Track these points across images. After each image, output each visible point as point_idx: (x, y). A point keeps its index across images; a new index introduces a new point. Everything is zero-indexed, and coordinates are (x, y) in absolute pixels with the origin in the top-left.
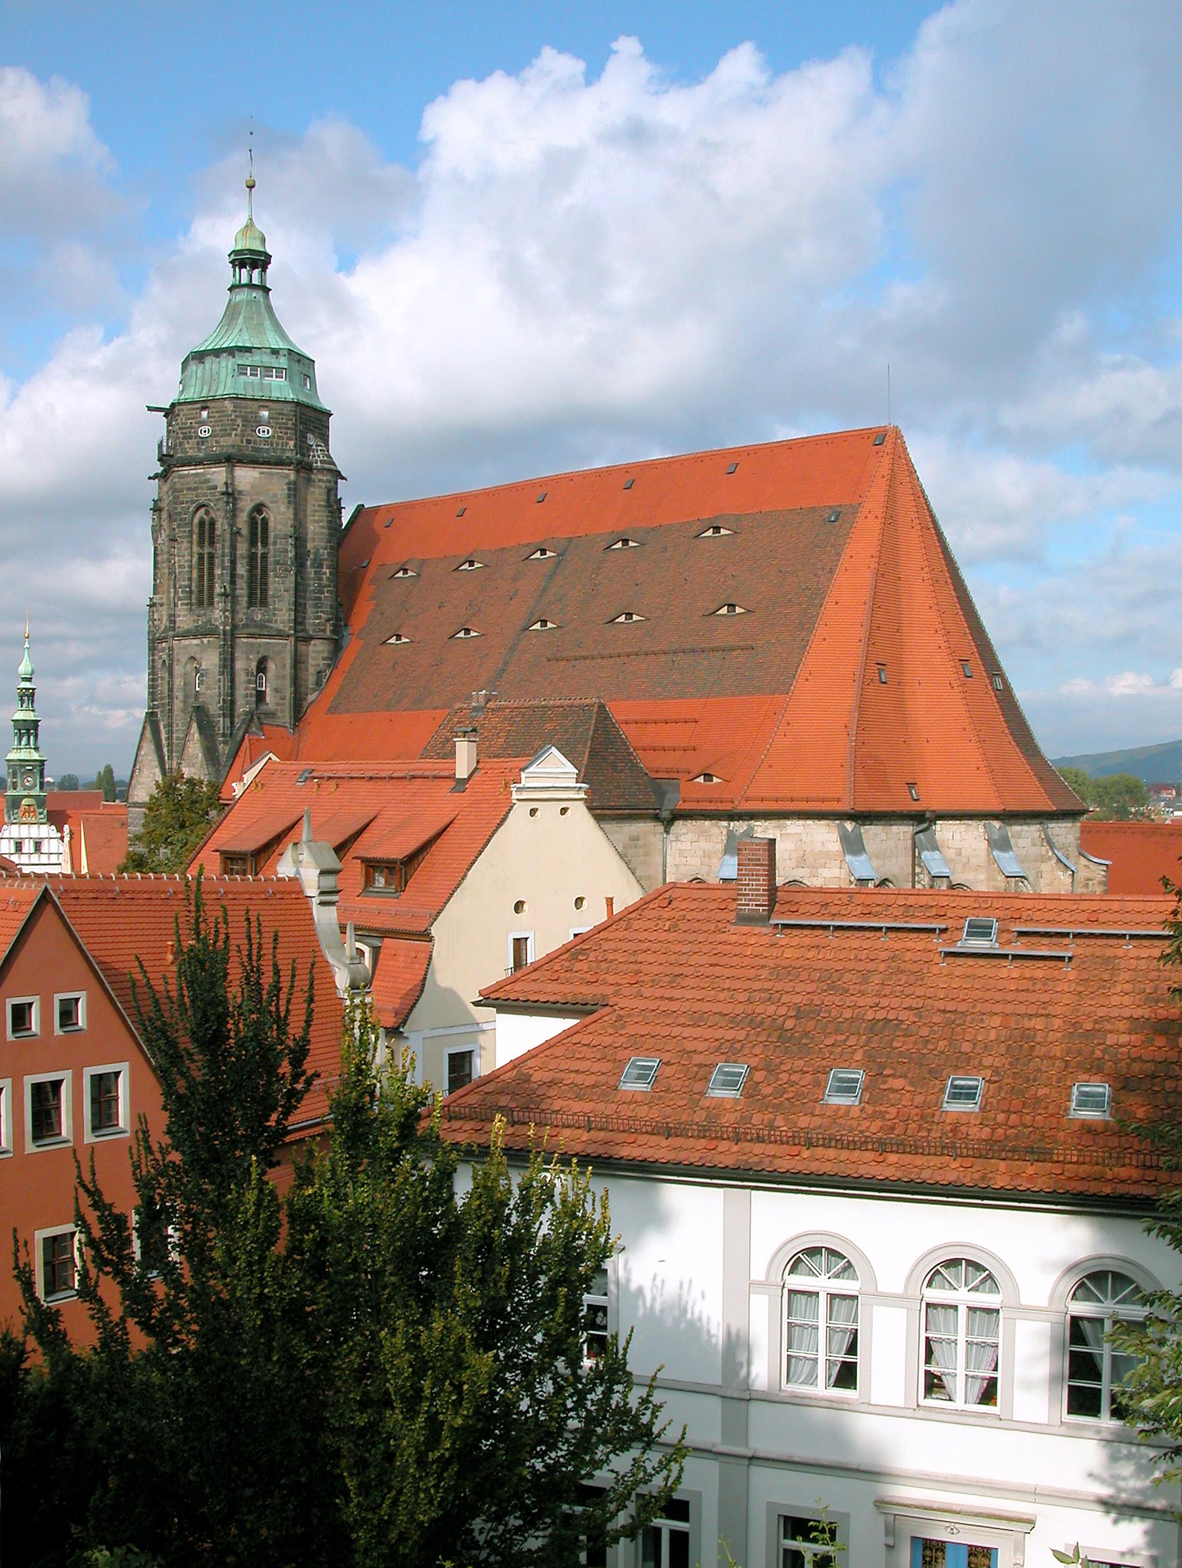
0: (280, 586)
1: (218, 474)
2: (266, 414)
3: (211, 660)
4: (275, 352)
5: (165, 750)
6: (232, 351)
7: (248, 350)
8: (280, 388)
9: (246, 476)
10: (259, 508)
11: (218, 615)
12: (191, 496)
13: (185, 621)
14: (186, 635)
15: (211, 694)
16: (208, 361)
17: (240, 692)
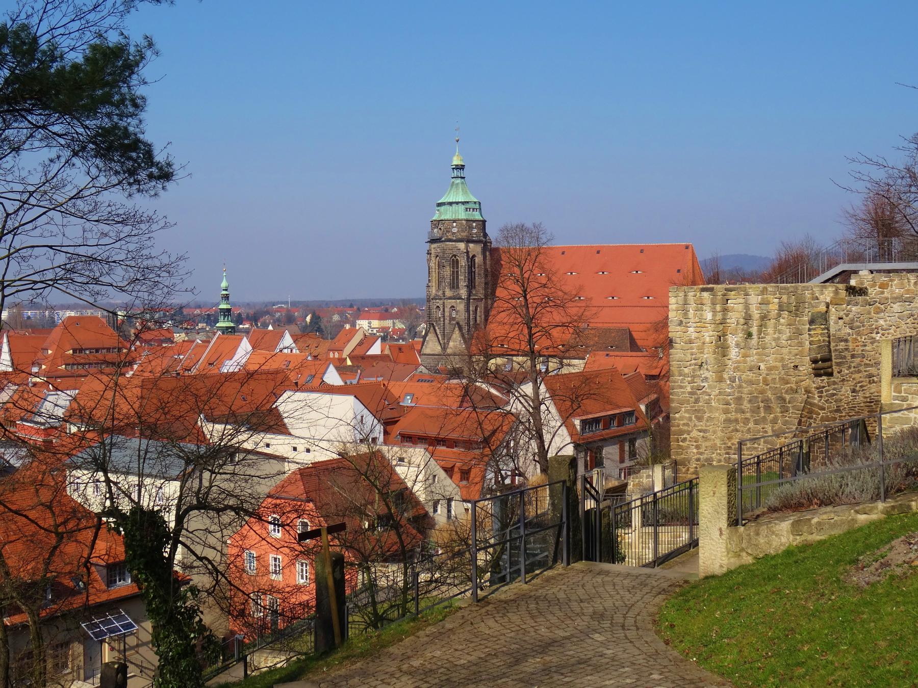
0: (479, 281)
1: (462, 246)
2: (474, 224)
3: (461, 307)
4: (475, 203)
5: (440, 336)
6: (463, 203)
7: (468, 202)
8: (478, 217)
9: (471, 245)
10: (474, 256)
11: (463, 292)
12: (451, 252)
13: (448, 293)
14: (450, 298)
15: (461, 316)
16: (454, 205)
17: (471, 317)
